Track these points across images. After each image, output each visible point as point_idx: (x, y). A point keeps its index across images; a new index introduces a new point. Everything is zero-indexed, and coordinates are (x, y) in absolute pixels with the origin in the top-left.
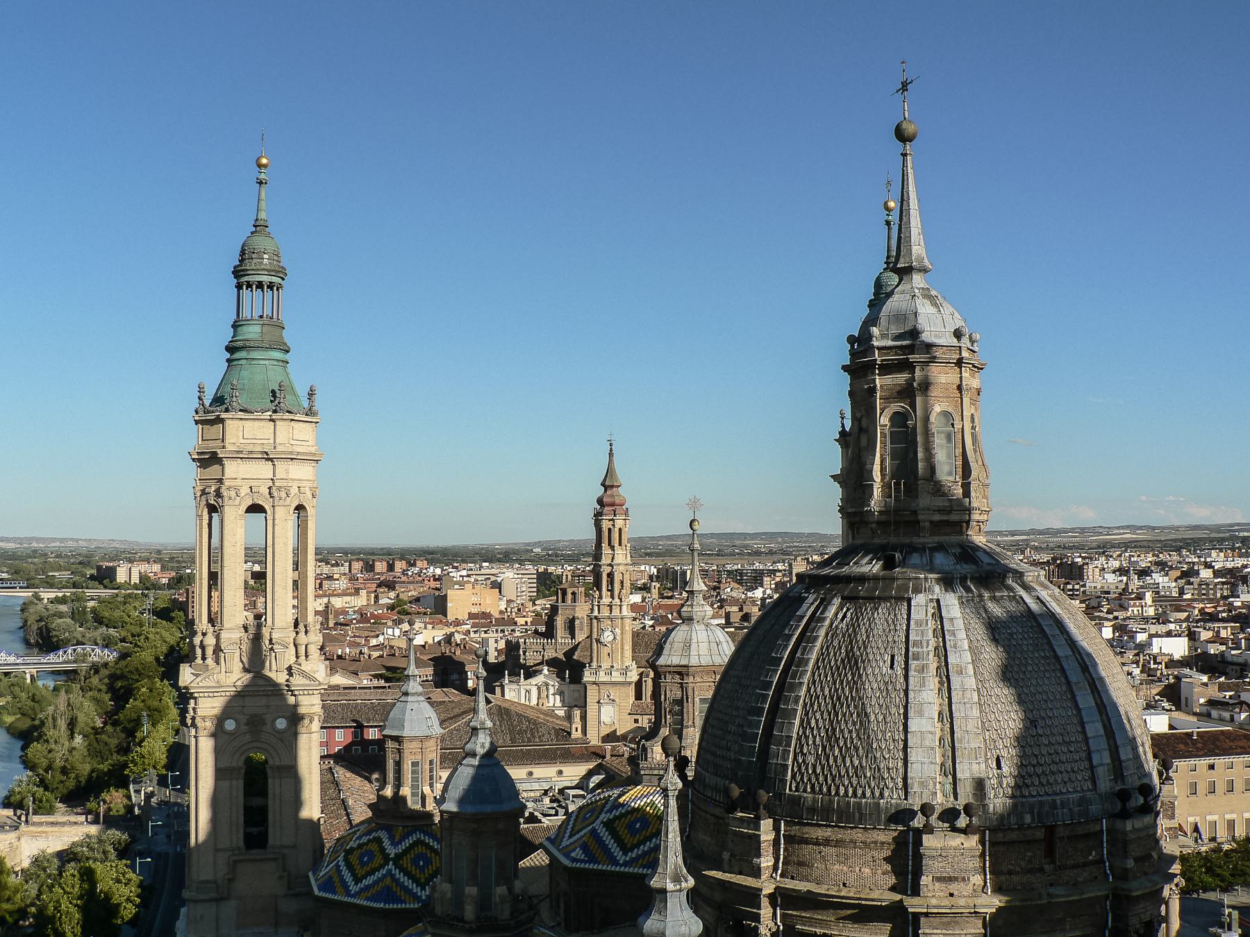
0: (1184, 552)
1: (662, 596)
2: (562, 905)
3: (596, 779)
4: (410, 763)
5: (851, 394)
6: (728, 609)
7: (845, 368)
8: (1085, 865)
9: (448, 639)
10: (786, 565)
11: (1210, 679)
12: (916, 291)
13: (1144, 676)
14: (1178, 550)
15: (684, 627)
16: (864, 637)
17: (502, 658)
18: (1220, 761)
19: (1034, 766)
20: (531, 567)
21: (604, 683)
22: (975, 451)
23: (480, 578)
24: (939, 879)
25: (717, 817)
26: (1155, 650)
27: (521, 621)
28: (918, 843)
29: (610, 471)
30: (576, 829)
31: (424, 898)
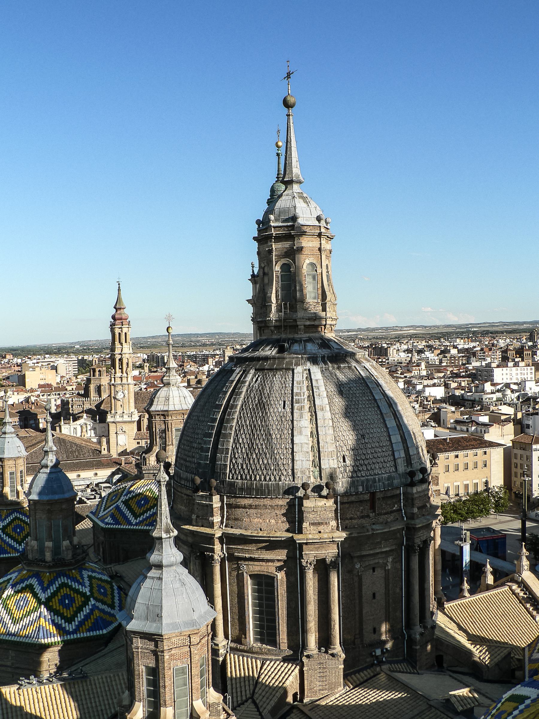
0: (442, 340)
1: (150, 371)
2: (101, 550)
3: (117, 477)
5: (258, 253)
6: (189, 377)
7: (255, 239)
8: (392, 512)
9: (27, 400)
10: (221, 351)
11: (456, 408)
12: (295, 194)
13: (421, 409)
14: (439, 339)
15: (165, 389)
17: (59, 410)
18: (461, 453)
19: (363, 460)
20: (74, 356)
21: (119, 422)
22: (329, 285)
23: (44, 364)
24: (313, 524)
25: (188, 495)
26: (427, 394)
27: (70, 388)
28: (301, 505)
29: (119, 300)
30: (107, 506)
31: (21, 550)
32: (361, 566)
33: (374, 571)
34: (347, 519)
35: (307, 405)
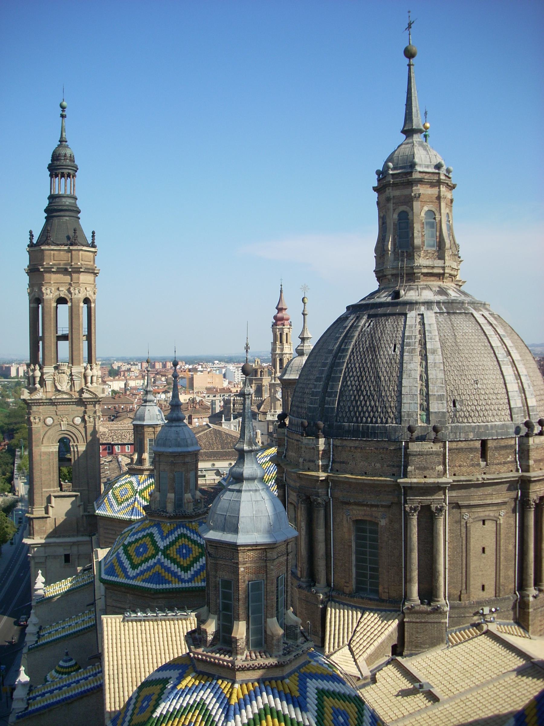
4: (148, 439)
16: (380, 335)
24: (418, 468)
28: (407, 447)
32: (470, 517)
33: (484, 524)
34: (456, 466)
35: (418, 348)
